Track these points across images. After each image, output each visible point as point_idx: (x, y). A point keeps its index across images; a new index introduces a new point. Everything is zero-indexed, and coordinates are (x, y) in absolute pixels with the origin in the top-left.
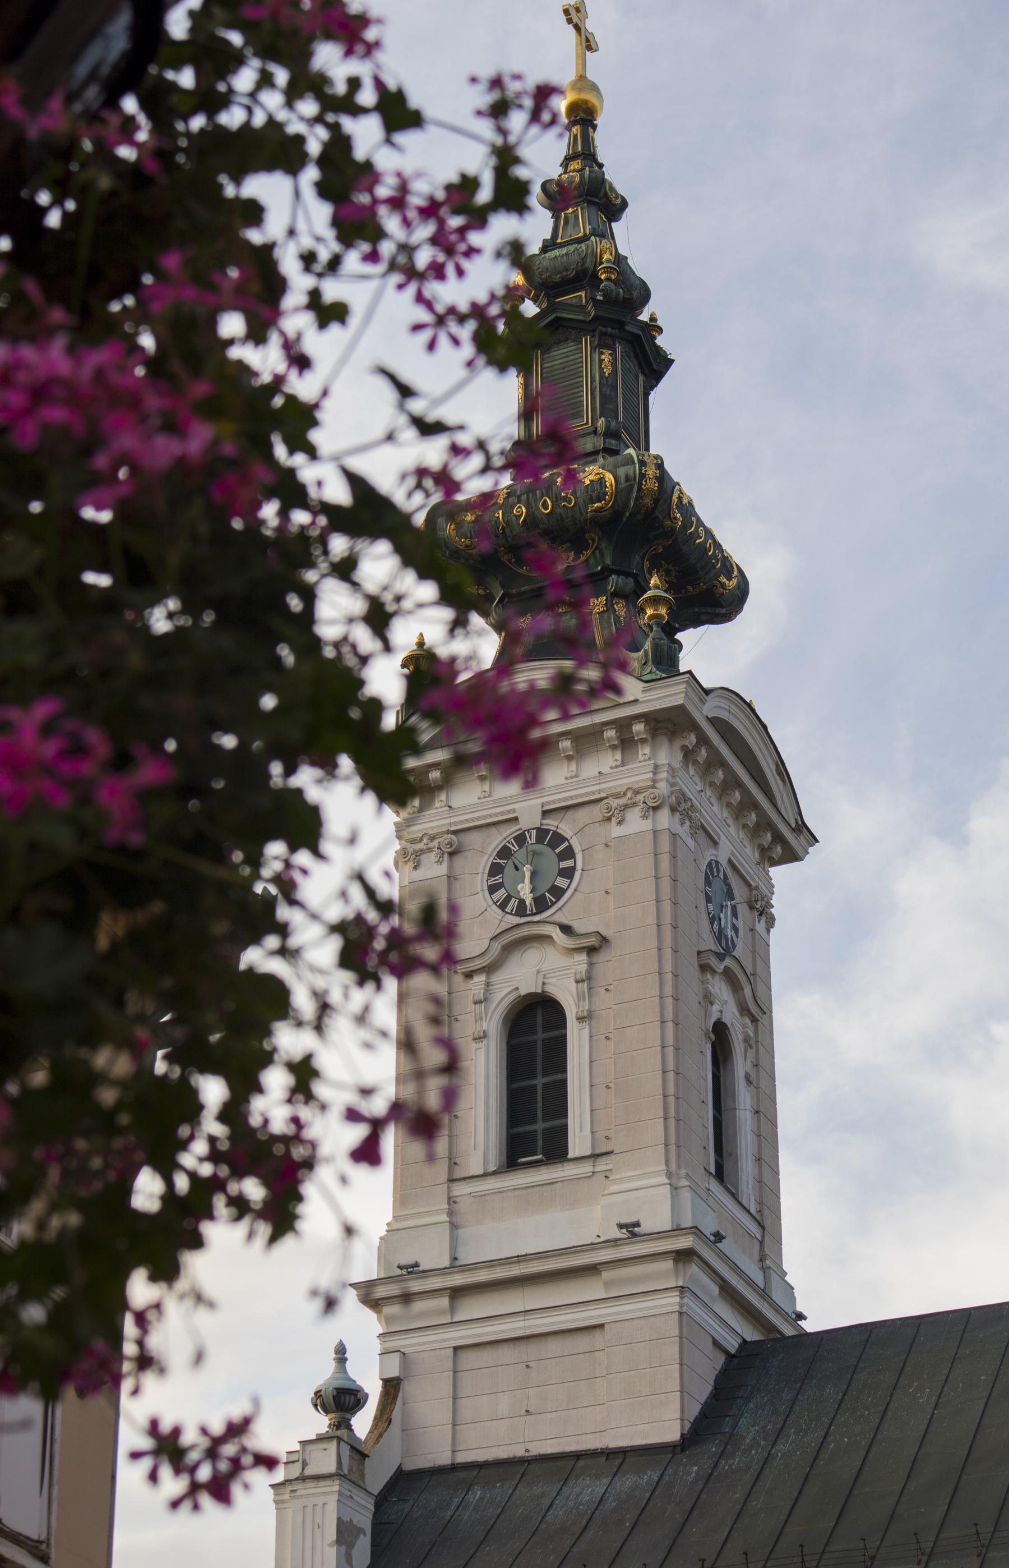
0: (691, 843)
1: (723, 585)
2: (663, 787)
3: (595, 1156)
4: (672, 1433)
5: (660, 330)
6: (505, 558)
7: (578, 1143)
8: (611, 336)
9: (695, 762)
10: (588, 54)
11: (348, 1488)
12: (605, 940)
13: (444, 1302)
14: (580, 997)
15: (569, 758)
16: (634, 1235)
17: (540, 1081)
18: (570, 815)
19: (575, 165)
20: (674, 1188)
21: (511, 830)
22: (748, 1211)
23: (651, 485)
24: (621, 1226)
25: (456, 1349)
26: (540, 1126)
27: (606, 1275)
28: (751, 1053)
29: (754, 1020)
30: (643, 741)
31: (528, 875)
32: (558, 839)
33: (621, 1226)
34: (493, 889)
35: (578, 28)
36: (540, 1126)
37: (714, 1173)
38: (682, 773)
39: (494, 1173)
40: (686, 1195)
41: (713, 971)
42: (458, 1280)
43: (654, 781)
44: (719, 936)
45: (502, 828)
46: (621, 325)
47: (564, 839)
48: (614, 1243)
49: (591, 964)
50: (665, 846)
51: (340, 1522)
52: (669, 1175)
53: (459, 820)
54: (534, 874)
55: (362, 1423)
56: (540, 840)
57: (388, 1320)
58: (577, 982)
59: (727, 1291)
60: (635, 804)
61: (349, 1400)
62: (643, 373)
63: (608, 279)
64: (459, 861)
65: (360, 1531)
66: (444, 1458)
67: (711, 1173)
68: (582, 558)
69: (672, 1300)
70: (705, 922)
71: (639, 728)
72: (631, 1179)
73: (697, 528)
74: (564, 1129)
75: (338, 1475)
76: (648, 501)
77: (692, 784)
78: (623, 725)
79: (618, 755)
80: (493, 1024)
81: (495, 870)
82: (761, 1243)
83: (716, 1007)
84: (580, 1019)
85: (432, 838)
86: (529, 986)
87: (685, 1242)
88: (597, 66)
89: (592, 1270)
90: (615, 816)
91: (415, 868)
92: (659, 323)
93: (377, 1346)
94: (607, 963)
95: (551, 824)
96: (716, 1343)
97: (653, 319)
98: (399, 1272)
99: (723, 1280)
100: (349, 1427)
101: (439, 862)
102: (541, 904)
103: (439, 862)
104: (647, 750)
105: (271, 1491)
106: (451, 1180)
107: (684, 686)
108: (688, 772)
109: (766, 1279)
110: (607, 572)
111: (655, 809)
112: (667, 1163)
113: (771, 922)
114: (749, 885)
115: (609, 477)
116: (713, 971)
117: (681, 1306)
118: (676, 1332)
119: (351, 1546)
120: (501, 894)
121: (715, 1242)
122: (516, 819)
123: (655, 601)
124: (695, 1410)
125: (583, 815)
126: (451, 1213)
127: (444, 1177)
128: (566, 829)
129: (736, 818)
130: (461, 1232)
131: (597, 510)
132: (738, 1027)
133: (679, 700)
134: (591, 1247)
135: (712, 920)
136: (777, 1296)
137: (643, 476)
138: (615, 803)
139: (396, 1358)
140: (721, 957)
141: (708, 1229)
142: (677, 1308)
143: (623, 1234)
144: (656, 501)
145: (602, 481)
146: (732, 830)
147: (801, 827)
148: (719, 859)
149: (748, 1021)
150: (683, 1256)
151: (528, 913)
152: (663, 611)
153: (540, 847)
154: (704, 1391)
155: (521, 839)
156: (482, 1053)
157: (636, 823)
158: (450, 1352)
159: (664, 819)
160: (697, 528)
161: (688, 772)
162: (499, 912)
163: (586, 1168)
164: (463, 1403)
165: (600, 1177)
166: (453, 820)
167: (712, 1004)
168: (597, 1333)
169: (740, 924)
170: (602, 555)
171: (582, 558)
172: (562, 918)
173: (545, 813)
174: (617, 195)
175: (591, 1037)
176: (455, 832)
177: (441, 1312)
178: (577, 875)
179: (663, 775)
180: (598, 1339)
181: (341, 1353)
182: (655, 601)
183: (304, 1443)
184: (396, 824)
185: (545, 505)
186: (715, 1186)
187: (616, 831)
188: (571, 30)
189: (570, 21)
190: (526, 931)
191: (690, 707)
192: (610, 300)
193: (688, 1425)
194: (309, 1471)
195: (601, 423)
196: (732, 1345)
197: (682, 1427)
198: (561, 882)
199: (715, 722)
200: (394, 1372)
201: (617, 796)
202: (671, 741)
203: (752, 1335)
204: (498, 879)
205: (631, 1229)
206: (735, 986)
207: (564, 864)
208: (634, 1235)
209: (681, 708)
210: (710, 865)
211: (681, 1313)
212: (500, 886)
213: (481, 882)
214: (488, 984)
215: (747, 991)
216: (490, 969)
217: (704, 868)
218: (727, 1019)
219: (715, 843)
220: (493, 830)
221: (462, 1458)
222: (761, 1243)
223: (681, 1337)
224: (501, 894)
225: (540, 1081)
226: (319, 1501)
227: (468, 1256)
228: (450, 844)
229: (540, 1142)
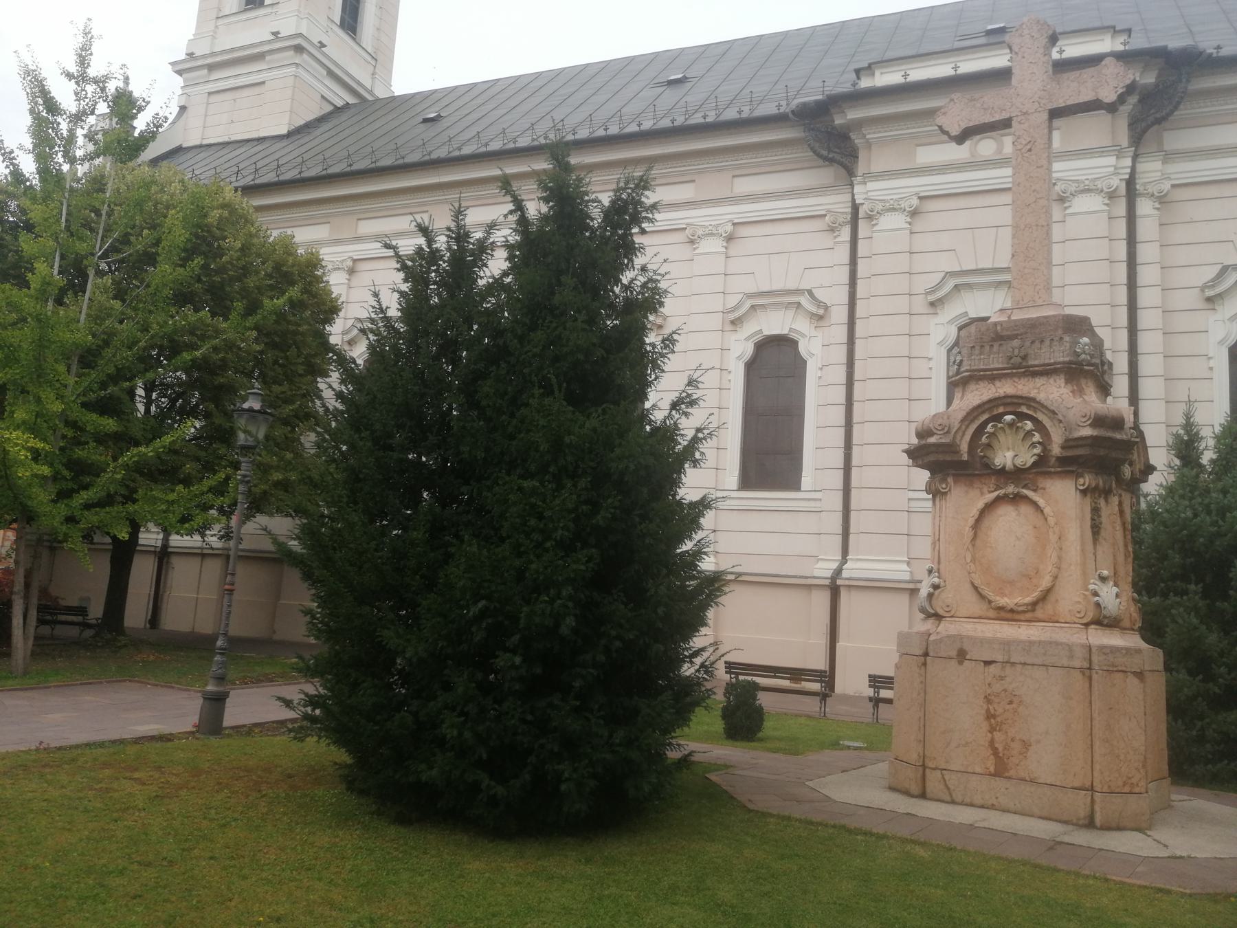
4: (285, 131)
13: (206, 71)
16: (278, 38)
24: (273, 33)
25: (210, 94)
27: (268, 58)
33: (273, 33)
42: (210, 61)
48: (269, 42)
59: (331, 74)
66: (198, 143)
89: (260, 57)
96: (322, 96)
99: (328, 68)
134: (261, 44)
143: (272, 37)
163: (268, 10)
196: (340, 103)
203: (351, 100)
205: (276, 34)
221: (205, 142)
222: (375, 67)
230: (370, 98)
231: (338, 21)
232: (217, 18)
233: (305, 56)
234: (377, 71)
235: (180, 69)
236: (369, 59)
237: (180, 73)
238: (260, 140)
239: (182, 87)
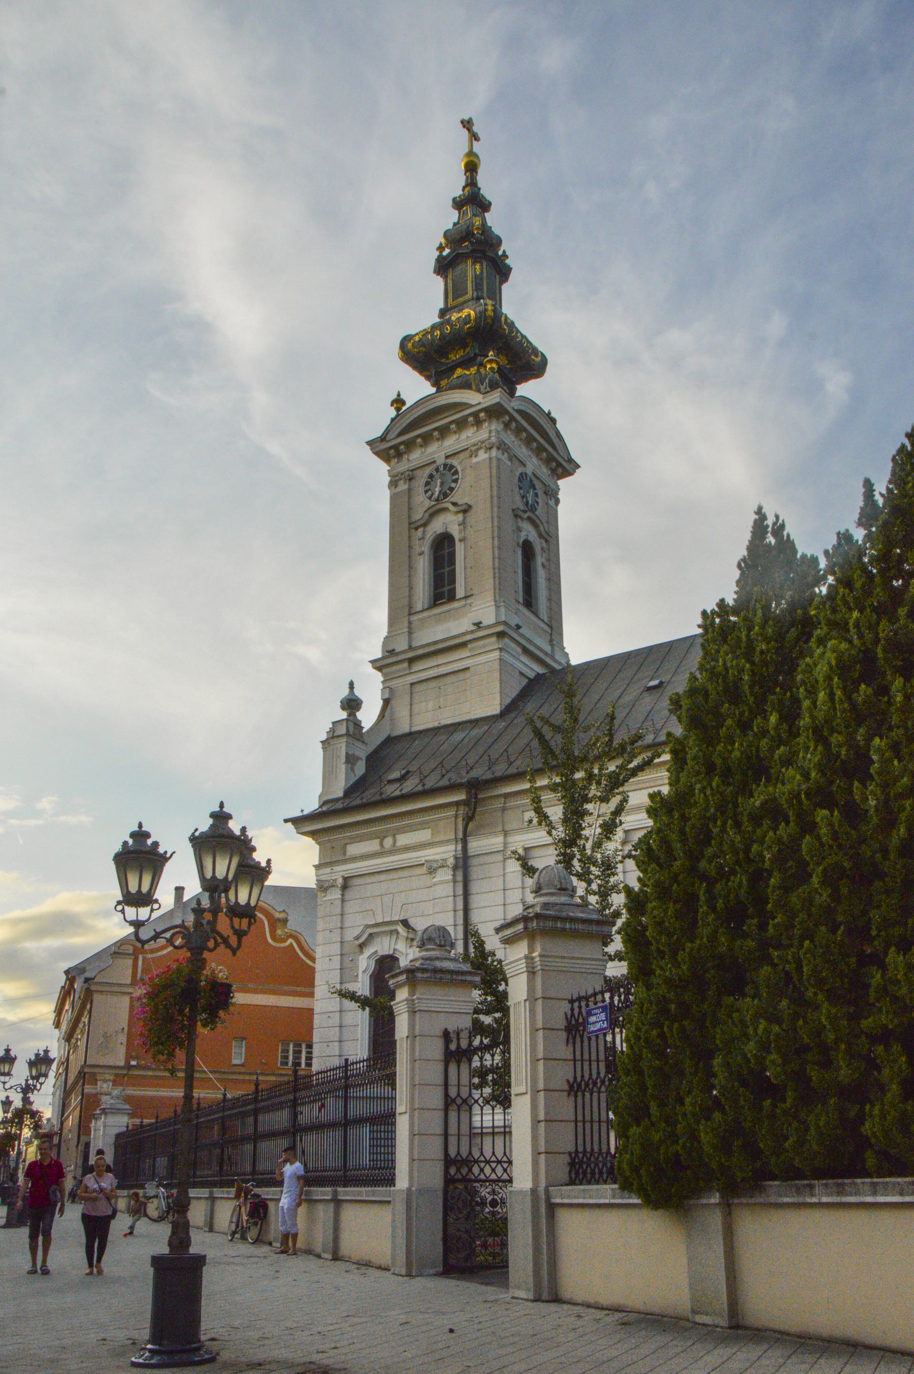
0: (509, 463)
1: (533, 360)
2: (493, 439)
3: (466, 597)
4: (496, 710)
5: (507, 257)
6: (435, 356)
7: (460, 593)
8: (479, 257)
9: (510, 429)
10: (474, 142)
11: (351, 740)
12: (470, 507)
13: (406, 665)
14: (460, 532)
15: (455, 432)
16: (480, 627)
17: (447, 569)
19: (466, 190)
20: (497, 607)
21: (433, 466)
22: (543, 621)
23: (490, 313)
24: (474, 624)
25: (412, 684)
26: (446, 588)
27: (469, 646)
28: (545, 555)
29: (546, 541)
30: (485, 420)
31: (439, 484)
32: (452, 467)
33: (474, 624)
34: (426, 492)
35: (469, 130)
36: (446, 588)
37: (522, 602)
38: (503, 433)
39: (426, 609)
40: (503, 610)
41: (522, 518)
42: (411, 655)
43: (490, 437)
44: (527, 504)
46: (483, 252)
48: (472, 632)
49: (465, 518)
50: (494, 464)
51: (347, 754)
52: (495, 601)
53: (414, 464)
54: (442, 484)
55: (368, 717)
56: (445, 469)
57: (384, 675)
58: (459, 525)
60: (481, 448)
61: (354, 704)
62: (498, 274)
63: (478, 233)
64: (413, 482)
65: (359, 759)
67: (519, 602)
68: (466, 351)
69: (496, 654)
70: (518, 498)
71: (482, 415)
72: (479, 605)
73: (517, 333)
74: (455, 588)
75: (348, 734)
76: (489, 321)
77: (510, 439)
78: (475, 415)
79: (475, 428)
80: (426, 547)
81: (427, 484)
82: (551, 634)
83: (523, 534)
84: (460, 541)
85: (402, 474)
87: (500, 628)
88: (477, 148)
90: (474, 454)
91: (396, 487)
92: (507, 253)
93: (381, 686)
94: (471, 517)
95: (449, 461)
96: (521, 673)
97: (504, 252)
98: (387, 654)
100: (355, 716)
101: (405, 484)
102: (446, 495)
103: (405, 484)
104: (486, 424)
105: (321, 744)
106: (410, 614)
107: (498, 394)
108: (507, 433)
109: (553, 650)
110: (476, 355)
111: (490, 448)
112: (495, 597)
113: (557, 501)
114: (545, 485)
115: (472, 313)
116: (520, 517)
117: (501, 656)
118: (498, 667)
119: (353, 764)
120: (430, 493)
121: (517, 629)
122: (435, 462)
124: (508, 701)
125: (461, 456)
126: (410, 628)
127: (406, 613)
128: (454, 462)
129: (537, 456)
130: (414, 635)
131: (469, 328)
132: (538, 543)
133: (498, 400)
134: (463, 634)
135: (523, 497)
136: (558, 657)
137: (486, 310)
138: (473, 448)
139: (387, 690)
140: (525, 512)
141: (513, 624)
142: (498, 657)
143: (473, 628)
144: (493, 321)
145: (469, 315)
146: (534, 460)
147: (570, 460)
148: (527, 472)
149: (543, 541)
150: (501, 635)
152: (494, 365)
153: (445, 472)
154: (514, 693)
155: (437, 470)
156: (422, 560)
157: (482, 456)
158: (409, 686)
159: (494, 452)
160: (517, 333)
161: (507, 433)
163: (463, 602)
164: (416, 708)
165: (468, 606)
167: (521, 531)
168: (467, 671)
169: (540, 501)
170: (474, 349)
171: (466, 351)
172: (453, 500)
174: (486, 200)
175: (465, 548)
176: (412, 471)
177: (404, 669)
178: (459, 481)
179: (493, 434)
180: (468, 674)
181: (351, 685)
182: (491, 361)
183: (333, 723)
184: (388, 471)
185: (447, 330)
186: (524, 610)
187: (474, 460)
188: (465, 131)
189: (464, 127)
190: (438, 507)
191: (502, 402)
192: (479, 242)
193: (504, 707)
194: (335, 735)
195: (475, 293)
196: (532, 675)
197: (501, 707)
198: (453, 485)
199: (518, 411)
200: (387, 696)
201: (475, 445)
202: (498, 420)
203: (540, 670)
205: (478, 625)
207: (454, 477)
208: (480, 627)
209: (499, 403)
210: (521, 474)
211: (500, 659)
212: (429, 490)
213: (421, 490)
214: (424, 532)
215: (541, 528)
216: (425, 525)
217: (518, 474)
218: (531, 539)
219: (524, 465)
220: (426, 467)
221: (414, 729)
222: (551, 634)
223: (500, 670)
225: (447, 569)
226: (339, 746)
227: (414, 645)
228: (409, 475)
229: (446, 595)
230: (558, 667)
231: (521, 600)
234: (553, 637)
235: (379, 665)
236: (547, 628)
237: (379, 669)
238: (475, 722)
239: (383, 682)
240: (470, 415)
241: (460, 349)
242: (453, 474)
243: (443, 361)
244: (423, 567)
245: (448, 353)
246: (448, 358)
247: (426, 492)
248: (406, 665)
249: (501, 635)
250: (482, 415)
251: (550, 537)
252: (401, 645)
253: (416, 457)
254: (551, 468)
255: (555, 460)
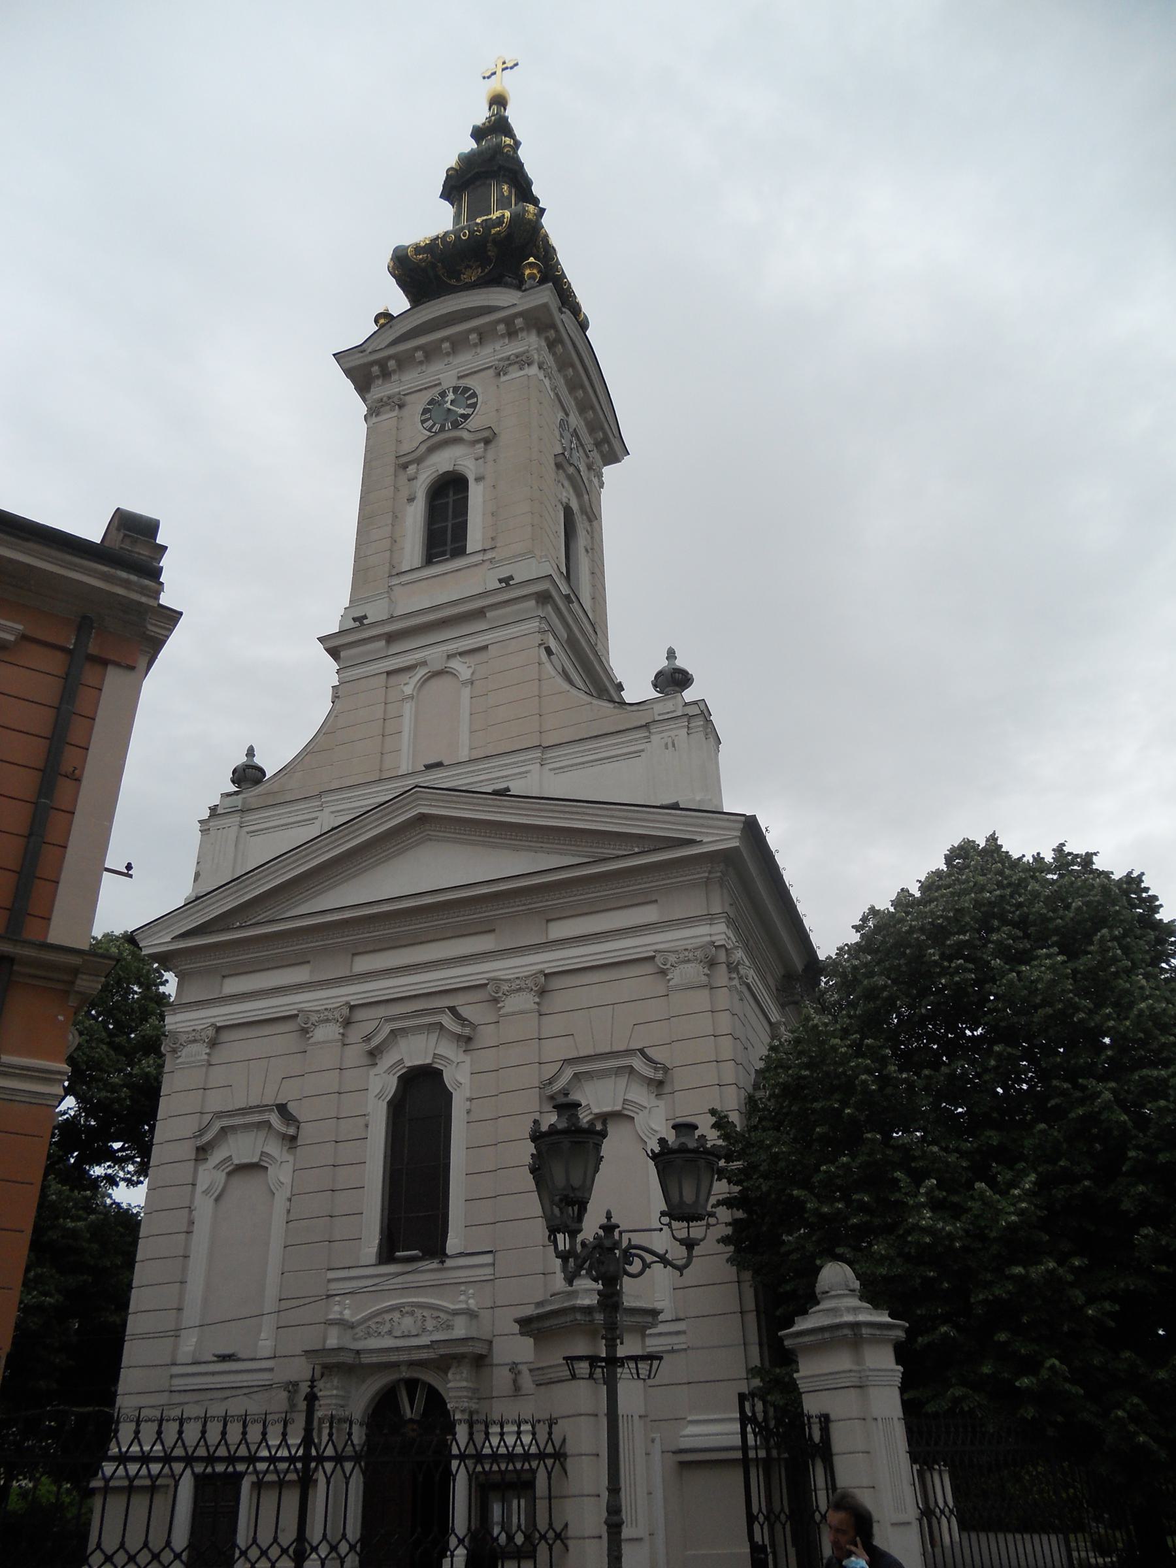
9: (554, 354)
13: (383, 643)
18: (476, 376)
21: (438, 389)
24: (500, 581)
25: (389, 673)
29: (590, 521)
30: (522, 329)
32: (467, 389)
34: (423, 422)
45: (430, 390)
47: (470, 389)
49: (485, 450)
71: (519, 322)
78: (509, 321)
81: (425, 411)
86: (446, 467)
89: (480, 613)
95: (463, 383)
120: (430, 423)
123: (531, 265)
131: (499, 233)
133: (544, 300)
150: (544, 598)
151: (447, 429)
162: (429, 433)
166: (401, 388)
171: (486, 270)
172: (467, 427)
173: (459, 378)
176: (404, 395)
187: (503, 379)
191: (550, 303)
202: (539, 333)
204: (428, 416)
205: (507, 581)
206: (579, 495)
207: (469, 402)
209: (545, 306)
213: (418, 418)
215: (586, 497)
216: (419, 461)
219: (567, 415)
224: (430, 423)
232: (390, 576)
233: (549, 608)
237: (334, 653)
240: (499, 321)
241: (477, 268)
242: (468, 398)
243: (453, 282)
244: (415, 516)
245: (460, 273)
246: (459, 280)
247: (423, 422)
248: (383, 643)
249: (544, 598)
250: (519, 322)
251: (593, 516)
252: (376, 612)
253: (409, 380)
254: (595, 439)
255: (602, 429)
